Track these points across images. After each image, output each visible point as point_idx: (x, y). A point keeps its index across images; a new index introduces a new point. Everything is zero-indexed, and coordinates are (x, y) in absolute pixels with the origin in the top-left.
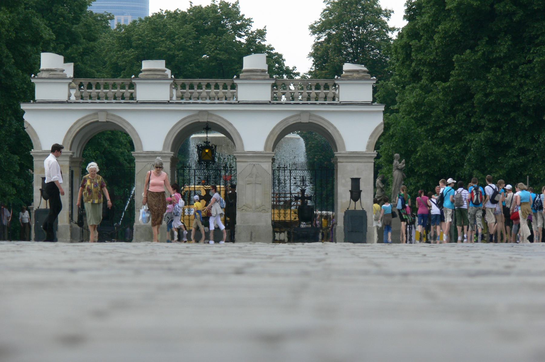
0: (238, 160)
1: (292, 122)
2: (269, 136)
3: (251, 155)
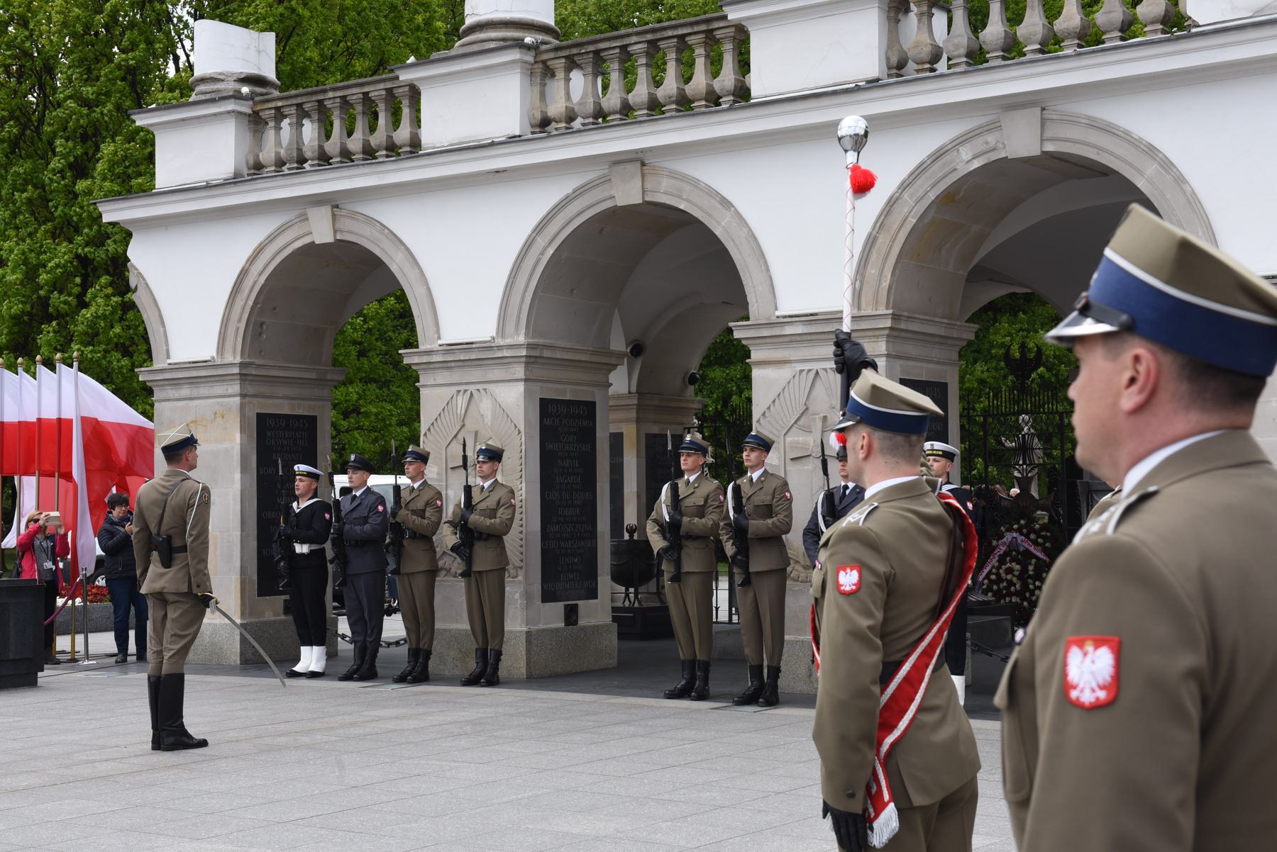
0: (756, 355)
1: (967, 161)
2: (871, 241)
3: (799, 329)
